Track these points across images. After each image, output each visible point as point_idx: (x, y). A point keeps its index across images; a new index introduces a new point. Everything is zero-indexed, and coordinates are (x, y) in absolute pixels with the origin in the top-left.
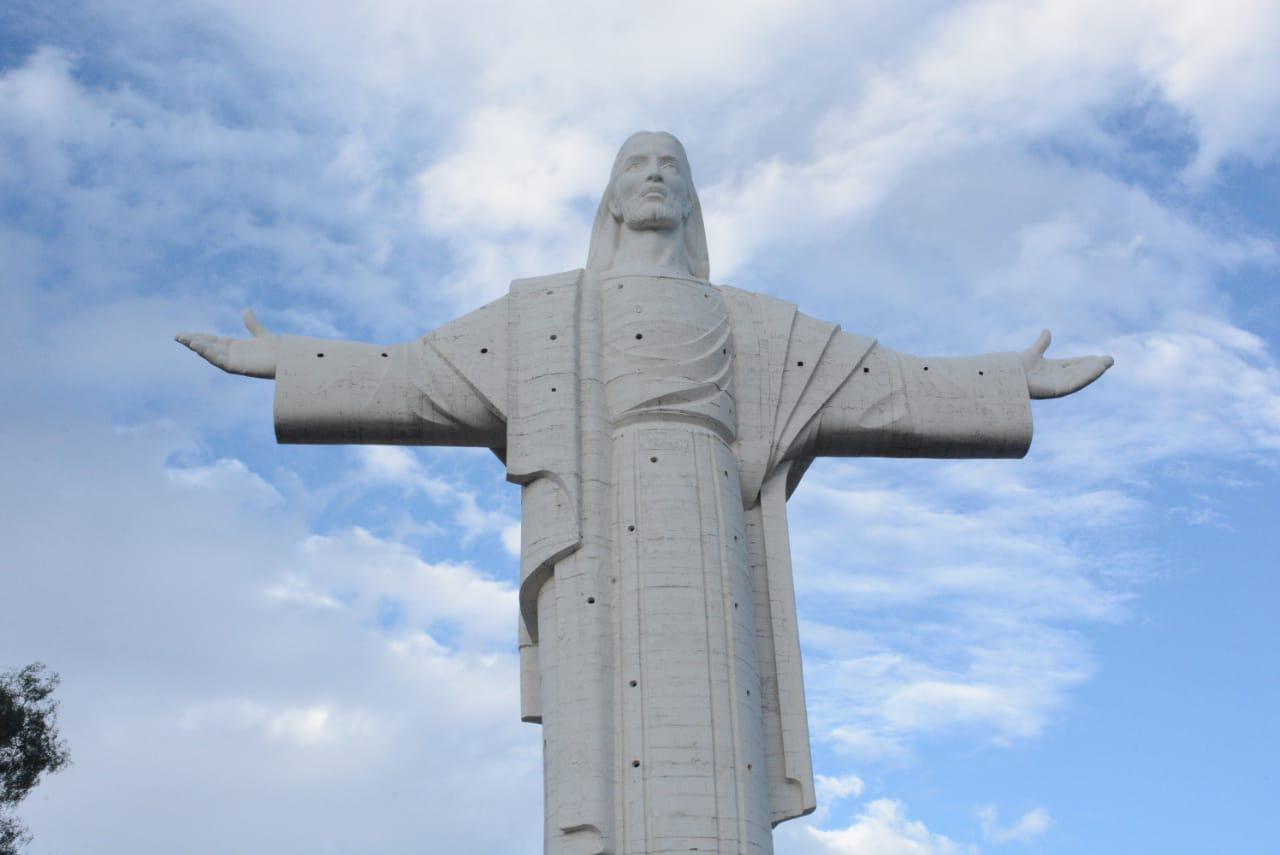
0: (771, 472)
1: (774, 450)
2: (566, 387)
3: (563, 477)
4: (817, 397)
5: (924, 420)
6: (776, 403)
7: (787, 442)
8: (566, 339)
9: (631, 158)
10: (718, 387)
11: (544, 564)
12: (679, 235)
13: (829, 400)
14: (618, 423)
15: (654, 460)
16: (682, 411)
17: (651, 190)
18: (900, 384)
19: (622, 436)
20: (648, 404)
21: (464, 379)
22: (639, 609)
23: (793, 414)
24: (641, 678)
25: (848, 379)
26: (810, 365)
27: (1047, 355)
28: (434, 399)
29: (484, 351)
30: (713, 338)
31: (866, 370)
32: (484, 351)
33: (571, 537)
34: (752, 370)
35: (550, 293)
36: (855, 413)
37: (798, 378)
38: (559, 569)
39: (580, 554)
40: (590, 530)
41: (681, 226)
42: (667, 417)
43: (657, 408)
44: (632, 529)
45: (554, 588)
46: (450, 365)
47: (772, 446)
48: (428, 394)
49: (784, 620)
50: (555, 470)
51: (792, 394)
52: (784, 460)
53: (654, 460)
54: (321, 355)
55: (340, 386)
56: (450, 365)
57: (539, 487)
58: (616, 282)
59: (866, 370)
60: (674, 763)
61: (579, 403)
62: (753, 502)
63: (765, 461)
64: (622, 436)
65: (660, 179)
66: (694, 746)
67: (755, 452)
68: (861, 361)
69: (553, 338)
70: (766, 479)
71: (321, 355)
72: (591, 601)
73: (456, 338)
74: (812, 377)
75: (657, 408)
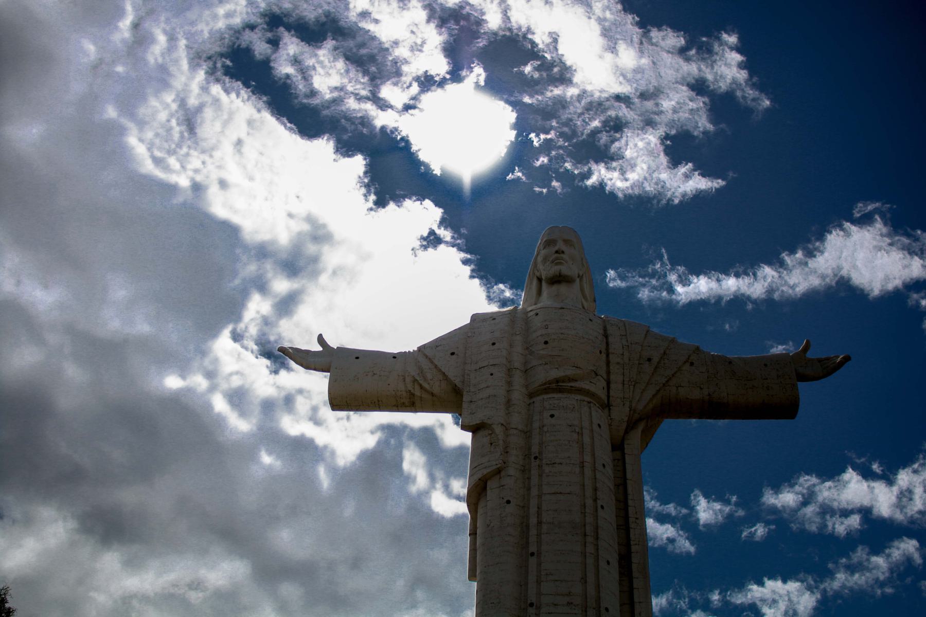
0: (631, 425)
3: (494, 427)
6: (633, 383)
7: (640, 407)
9: (545, 241)
11: (479, 479)
13: (667, 381)
15: (552, 416)
16: (571, 387)
17: (557, 259)
19: (534, 402)
20: (550, 382)
21: (440, 370)
22: (538, 508)
24: (538, 551)
26: (656, 360)
27: (809, 355)
28: (421, 382)
29: (453, 354)
32: (453, 354)
33: (497, 462)
34: (618, 363)
35: (494, 319)
39: (503, 473)
42: (560, 390)
44: (536, 458)
45: (486, 495)
46: (432, 362)
47: (630, 410)
48: (418, 379)
49: (637, 518)
50: (489, 422)
52: (640, 420)
53: (552, 416)
54: (357, 358)
55: (367, 375)
56: (432, 362)
57: (481, 433)
58: (535, 312)
60: (555, 605)
61: (509, 383)
63: (626, 419)
64: (534, 402)
65: (563, 252)
66: (569, 594)
67: (620, 413)
69: (494, 344)
70: (627, 432)
71: (357, 358)
72: (508, 502)
74: (656, 367)
75: (556, 386)
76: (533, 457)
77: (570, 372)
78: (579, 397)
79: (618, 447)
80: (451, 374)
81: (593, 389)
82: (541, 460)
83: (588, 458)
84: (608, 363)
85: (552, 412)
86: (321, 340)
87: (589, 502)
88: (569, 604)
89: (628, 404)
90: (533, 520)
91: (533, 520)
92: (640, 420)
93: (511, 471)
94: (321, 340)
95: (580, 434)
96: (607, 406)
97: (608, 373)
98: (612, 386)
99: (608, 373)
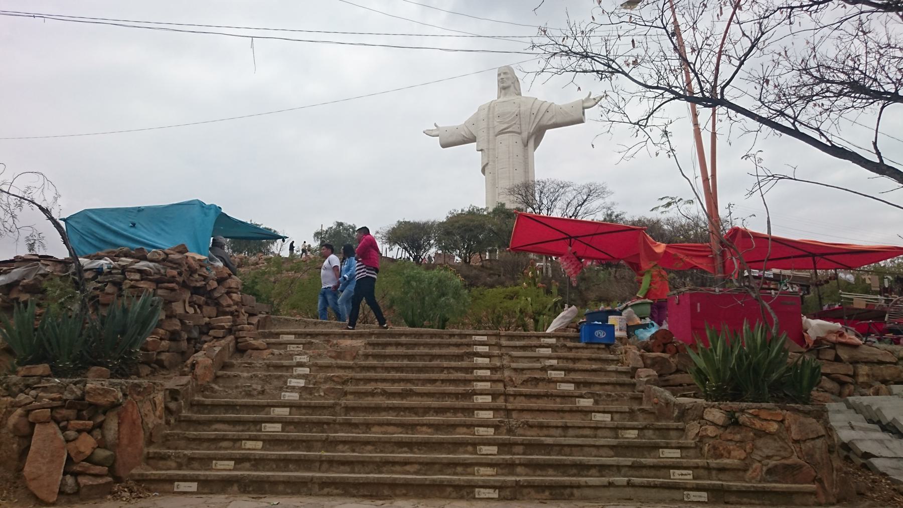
4: (537, 120)
5: (559, 120)
10: (515, 124)
12: (512, 88)
14: (496, 136)
25: (543, 115)
26: (535, 114)
30: (514, 113)
36: (545, 121)
37: (533, 117)
38: (486, 168)
40: (490, 159)
41: (512, 85)
43: (502, 132)
51: (532, 121)
52: (533, 134)
62: (526, 145)
67: (525, 135)
74: (536, 116)
75: (502, 132)
77: (505, 126)
78: (508, 134)
79: (526, 145)
80: (473, 133)
81: (514, 130)
83: (511, 155)
86: (436, 125)
87: (511, 169)
90: (497, 177)
91: (497, 177)
92: (531, 136)
93: (490, 163)
94: (436, 125)
95: (509, 147)
96: (520, 134)
99: (520, 121)
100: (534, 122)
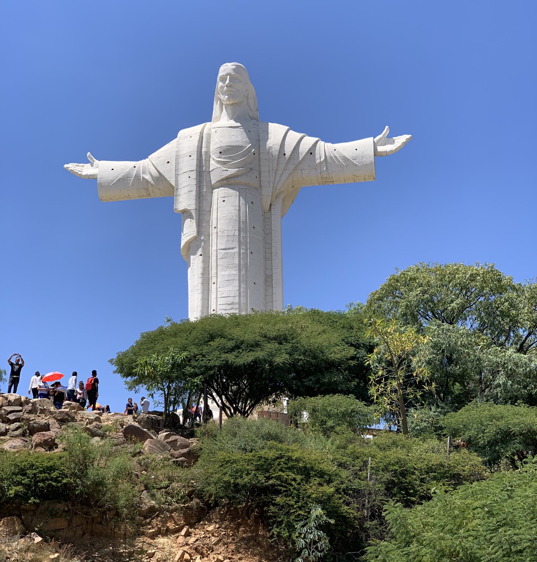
1: (274, 189)
2: (194, 175)
6: (275, 171)
8: (194, 157)
15: (224, 201)
18: (323, 158)
20: (223, 180)
23: (282, 174)
29: (168, 162)
31: (311, 153)
32: (168, 162)
35: (191, 137)
43: (226, 182)
53: (224, 201)
54: (113, 169)
59: (311, 153)
68: (309, 150)
69: (190, 156)
73: (159, 158)
75: (226, 182)
76: (213, 227)
82: (217, 228)
84: (259, 159)
85: (224, 199)
88: (232, 309)
89: (272, 185)
97: (259, 166)
98: (262, 174)
100: (285, 169)
